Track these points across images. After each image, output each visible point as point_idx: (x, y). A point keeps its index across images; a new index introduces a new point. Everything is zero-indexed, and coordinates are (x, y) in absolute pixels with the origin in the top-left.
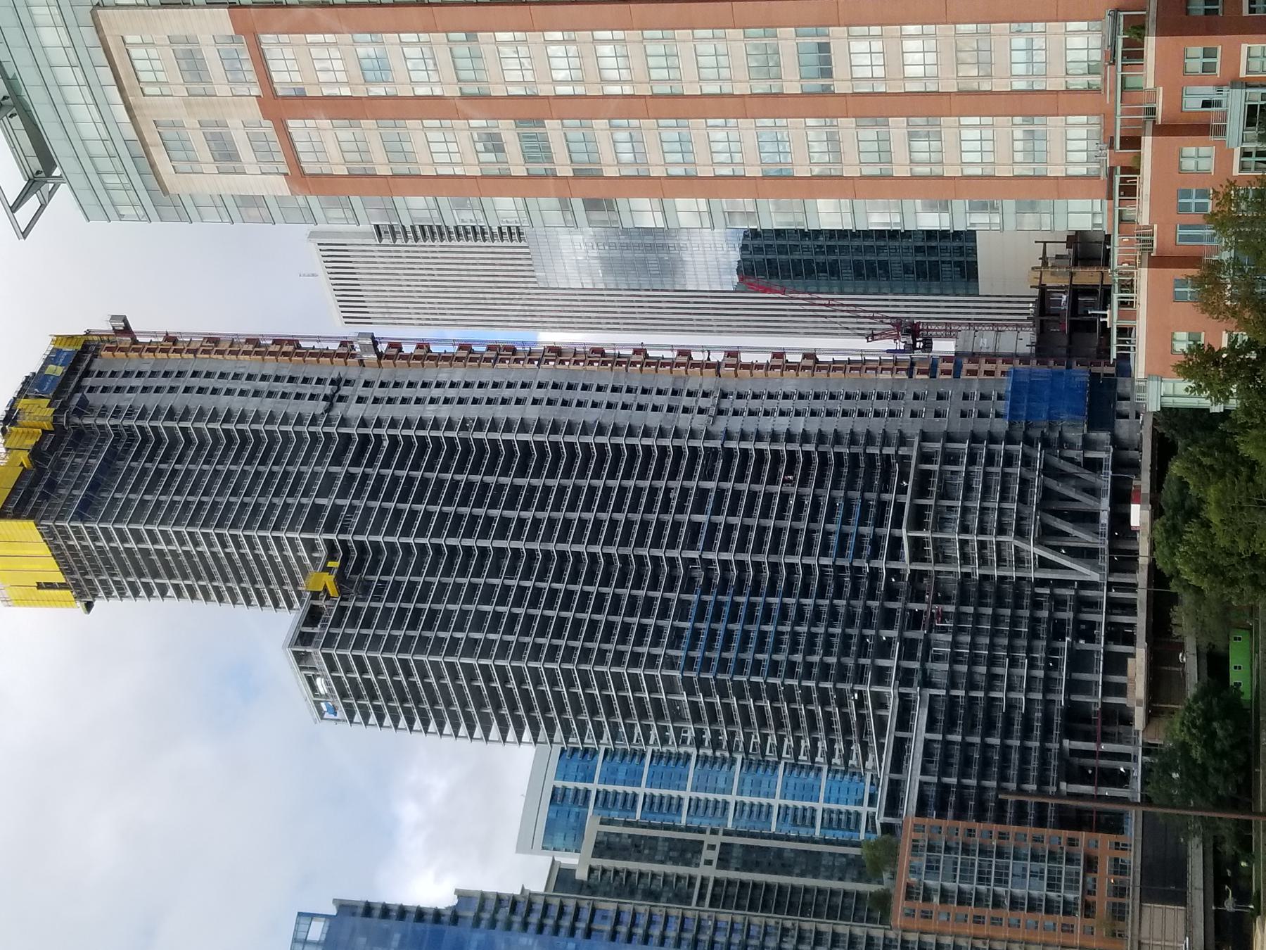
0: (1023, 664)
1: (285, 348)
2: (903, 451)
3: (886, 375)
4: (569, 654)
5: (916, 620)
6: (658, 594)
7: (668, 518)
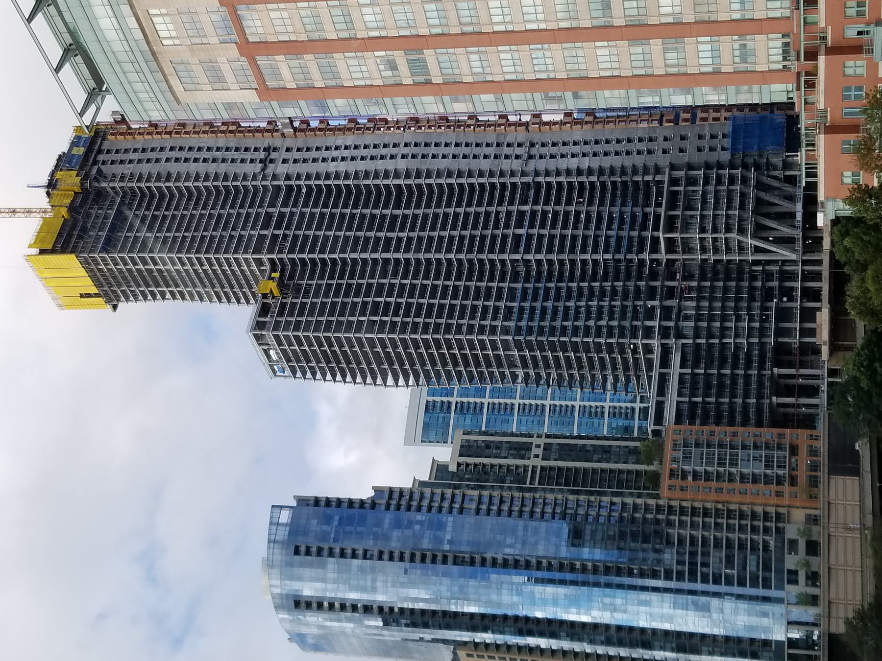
0: (745, 319)
1: (231, 128)
2: (658, 178)
5: (671, 293)
6: (494, 285)
7: (499, 232)
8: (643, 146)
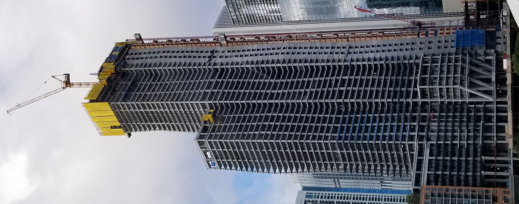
1: (195, 42)
3: (410, 37)
4: (296, 137)
5: (424, 119)
6: (328, 116)
7: (331, 89)
8: (409, 47)
